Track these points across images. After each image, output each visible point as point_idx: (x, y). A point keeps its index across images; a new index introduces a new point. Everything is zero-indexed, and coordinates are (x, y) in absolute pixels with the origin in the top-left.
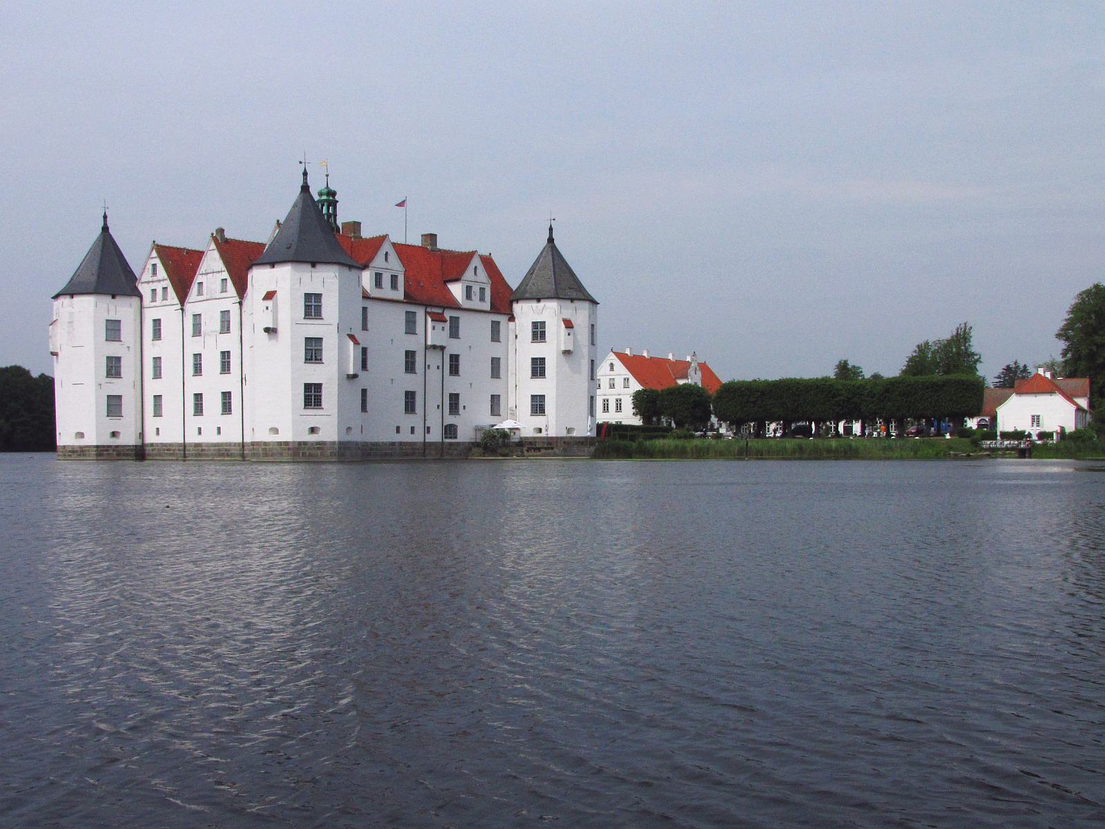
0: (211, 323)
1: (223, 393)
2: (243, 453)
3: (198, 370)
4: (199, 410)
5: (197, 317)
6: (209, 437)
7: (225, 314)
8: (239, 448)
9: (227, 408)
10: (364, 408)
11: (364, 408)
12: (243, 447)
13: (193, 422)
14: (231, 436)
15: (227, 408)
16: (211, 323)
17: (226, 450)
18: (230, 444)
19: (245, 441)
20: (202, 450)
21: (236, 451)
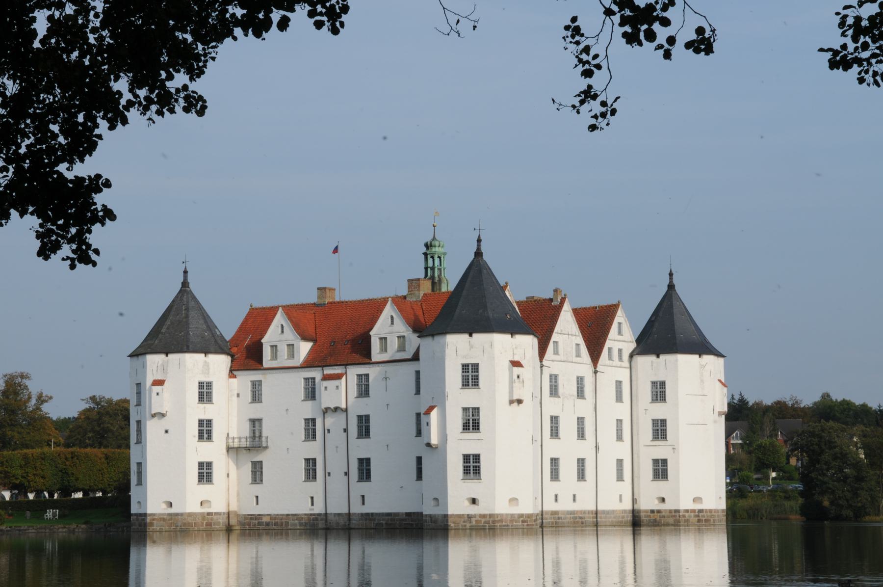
0: (568, 387)
1: (618, 460)
2: (597, 521)
3: (555, 433)
4: (555, 475)
5: (554, 378)
6: (565, 505)
7: (580, 381)
8: (592, 516)
9: (581, 475)
10: (419, 476)
11: (419, 476)
12: (596, 513)
13: (551, 488)
14: (586, 504)
15: (581, 475)
16: (568, 387)
17: (581, 518)
18: (584, 512)
19: (598, 509)
20: (559, 518)
21: (590, 519)
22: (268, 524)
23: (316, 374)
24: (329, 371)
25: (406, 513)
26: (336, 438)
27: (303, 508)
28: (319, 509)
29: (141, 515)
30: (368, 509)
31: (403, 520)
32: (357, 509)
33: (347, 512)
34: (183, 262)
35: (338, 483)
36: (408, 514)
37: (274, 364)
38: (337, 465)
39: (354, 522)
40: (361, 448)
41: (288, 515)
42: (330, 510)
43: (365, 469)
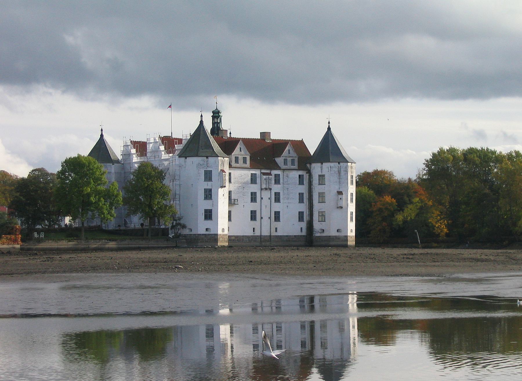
22: (233, 240)
23: (257, 172)
24: (263, 171)
25: (294, 236)
26: (266, 201)
27: (250, 233)
28: (257, 233)
29: (215, 234)
30: (279, 233)
31: (293, 238)
32: (274, 234)
33: (269, 235)
34: (201, 111)
35: (266, 222)
36: (295, 236)
37: (237, 165)
38: (266, 214)
39: (273, 239)
40: (277, 207)
41: (243, 236)
42: (263, 234)
43: (277, 216)
